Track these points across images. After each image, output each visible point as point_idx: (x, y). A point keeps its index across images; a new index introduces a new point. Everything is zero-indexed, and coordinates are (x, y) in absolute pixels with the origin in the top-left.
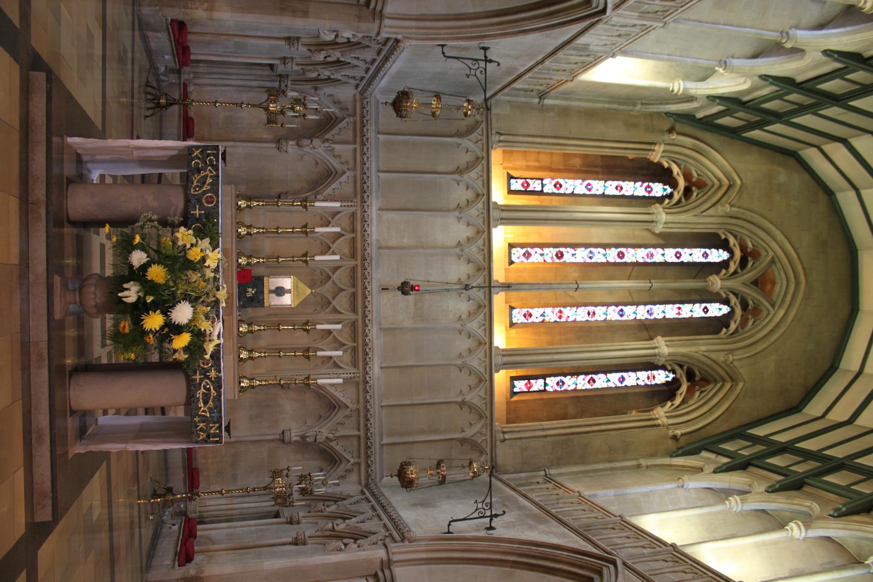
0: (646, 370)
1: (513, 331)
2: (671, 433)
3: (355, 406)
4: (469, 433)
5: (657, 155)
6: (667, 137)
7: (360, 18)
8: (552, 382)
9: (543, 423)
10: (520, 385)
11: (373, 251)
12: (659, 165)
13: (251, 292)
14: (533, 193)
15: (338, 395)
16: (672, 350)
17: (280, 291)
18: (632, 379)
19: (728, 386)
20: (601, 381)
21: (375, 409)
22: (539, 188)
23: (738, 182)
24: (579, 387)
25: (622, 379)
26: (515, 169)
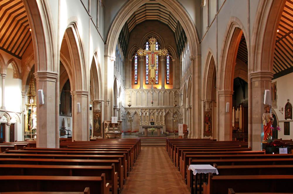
0: (167, 59)
1: (159, 84)
2: (176, 59)
3: (168, 110)
4: (174, 93)
5: (131, 60)
6: (128, 59)
7: (120, 111)
8: (168, 77)
9: (173, 80)
10: (168, 82)
11: (147, 107)
12: (132, 59)
13: (152, 123)
14: (137, 80)
15: (167, 112)
16: (163, 58)
17: (152, 120)
18: (168, 62)
19: (169, 47)
20: (168, 68)
21: (169, 107)
22: (136, 79)
23: (135, 45)
24: (169, 72)
25: (168, 64)
26: (133, 83)
